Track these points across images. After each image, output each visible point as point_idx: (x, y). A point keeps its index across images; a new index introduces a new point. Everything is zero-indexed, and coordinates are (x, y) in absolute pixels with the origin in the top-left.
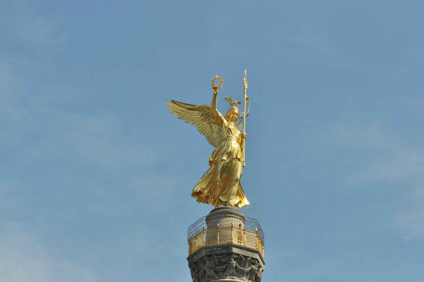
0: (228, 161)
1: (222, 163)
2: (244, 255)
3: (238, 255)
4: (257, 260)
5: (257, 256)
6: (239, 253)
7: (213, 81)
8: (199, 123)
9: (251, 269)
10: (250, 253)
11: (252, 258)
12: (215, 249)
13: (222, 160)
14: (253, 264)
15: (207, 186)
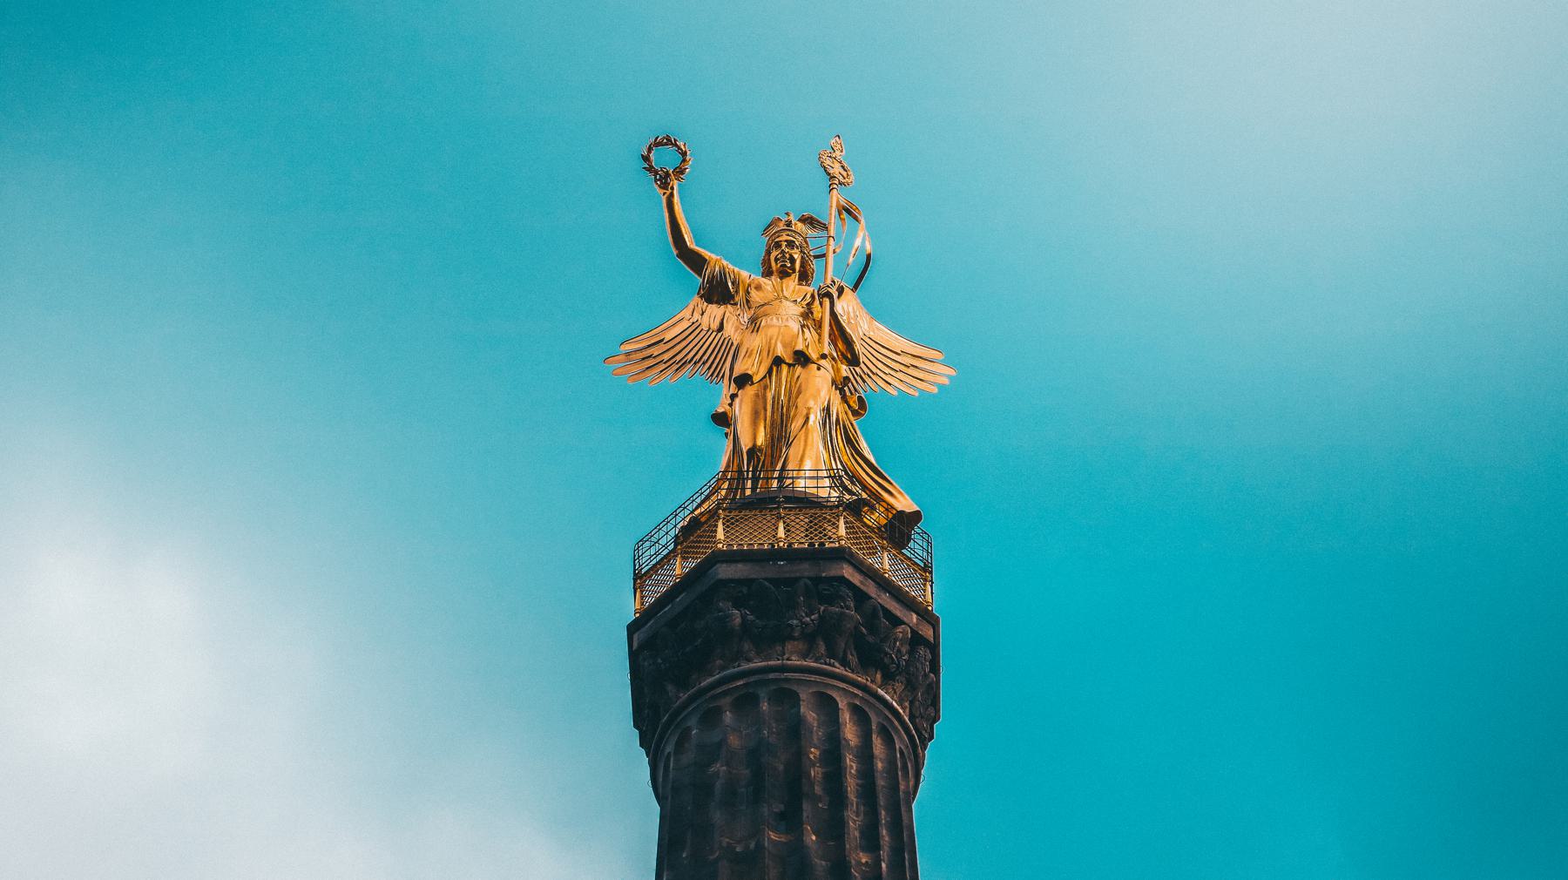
3: (748, 582)
7: (646, 159)
11: (817, 580)
14: (830, 600)
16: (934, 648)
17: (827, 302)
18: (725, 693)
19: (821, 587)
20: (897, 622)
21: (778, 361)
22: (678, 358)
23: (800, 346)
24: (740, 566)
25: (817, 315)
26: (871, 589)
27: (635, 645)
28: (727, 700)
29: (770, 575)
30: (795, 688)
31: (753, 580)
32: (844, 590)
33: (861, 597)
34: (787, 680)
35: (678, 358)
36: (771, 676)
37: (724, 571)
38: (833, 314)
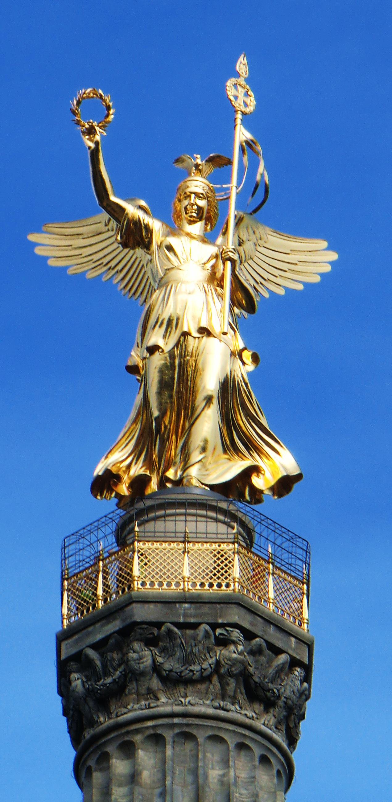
0: (167, 349)
1: (157, 360)
2: (181, 620)
3: (159, 625)
4: (236, 626)
5: (235, 615)
6: (163, 620)
7: (74, 113)
8: (119, 267)
9: (218, 663)
10: (206, 609)
11: (214, 626)
12: (90, 629)
13: (152, 350)
14: (224, 642)
15: (137, 452)
16: (308, 669)
17: (228, 264)
18: (137, 731)
19: (218, 631)
20: (278, 651)
21: (185, 334)
22: (96, 257)
23: (204, 324)
24: (152, 606)
25: (219, 275)
26: (258, 627)
27: (63, 657)
28: (138, 738)
29: (175, 620)
30: (194, 732)
31: (162, 624)
32: (236, 634)
33: (249, 635)
34: (188, 725)
35: (96, 257)
36: (176, 720)
37: (141, 613)
38: (235, 276)
